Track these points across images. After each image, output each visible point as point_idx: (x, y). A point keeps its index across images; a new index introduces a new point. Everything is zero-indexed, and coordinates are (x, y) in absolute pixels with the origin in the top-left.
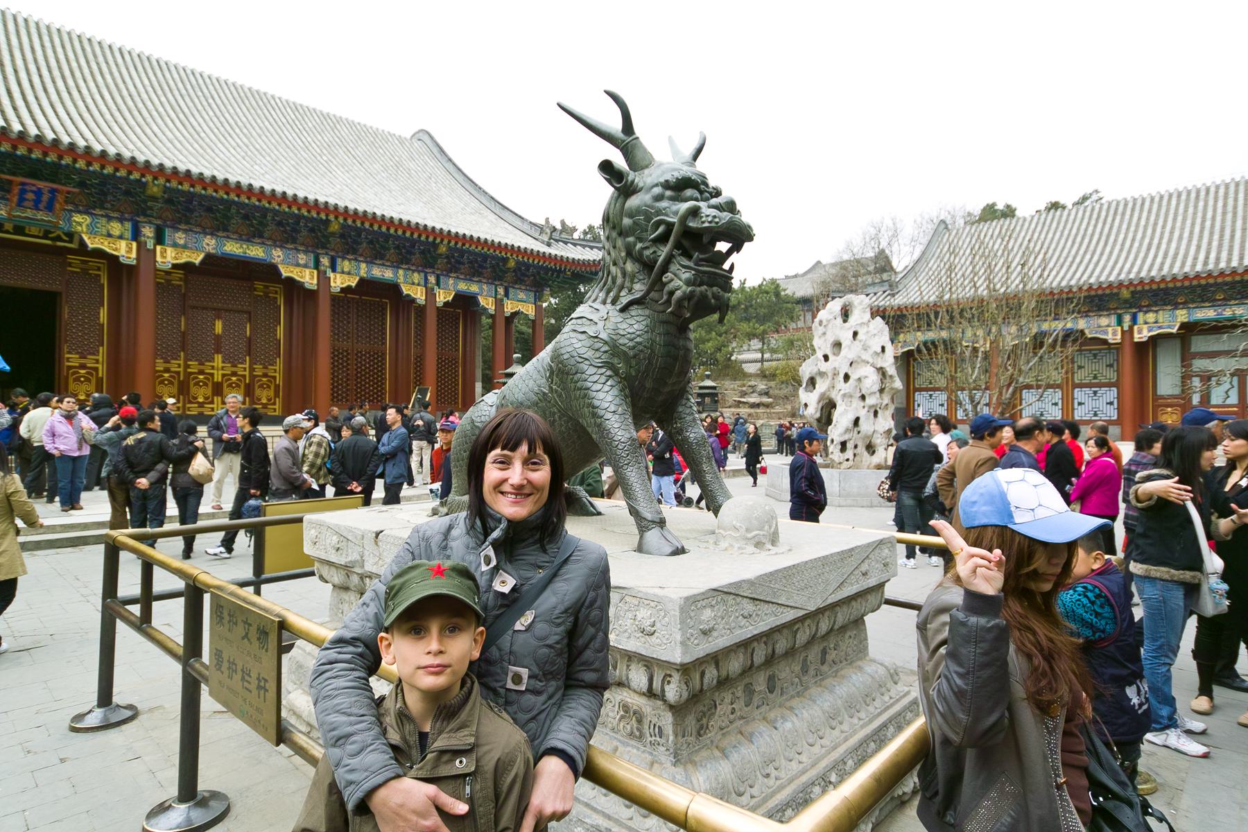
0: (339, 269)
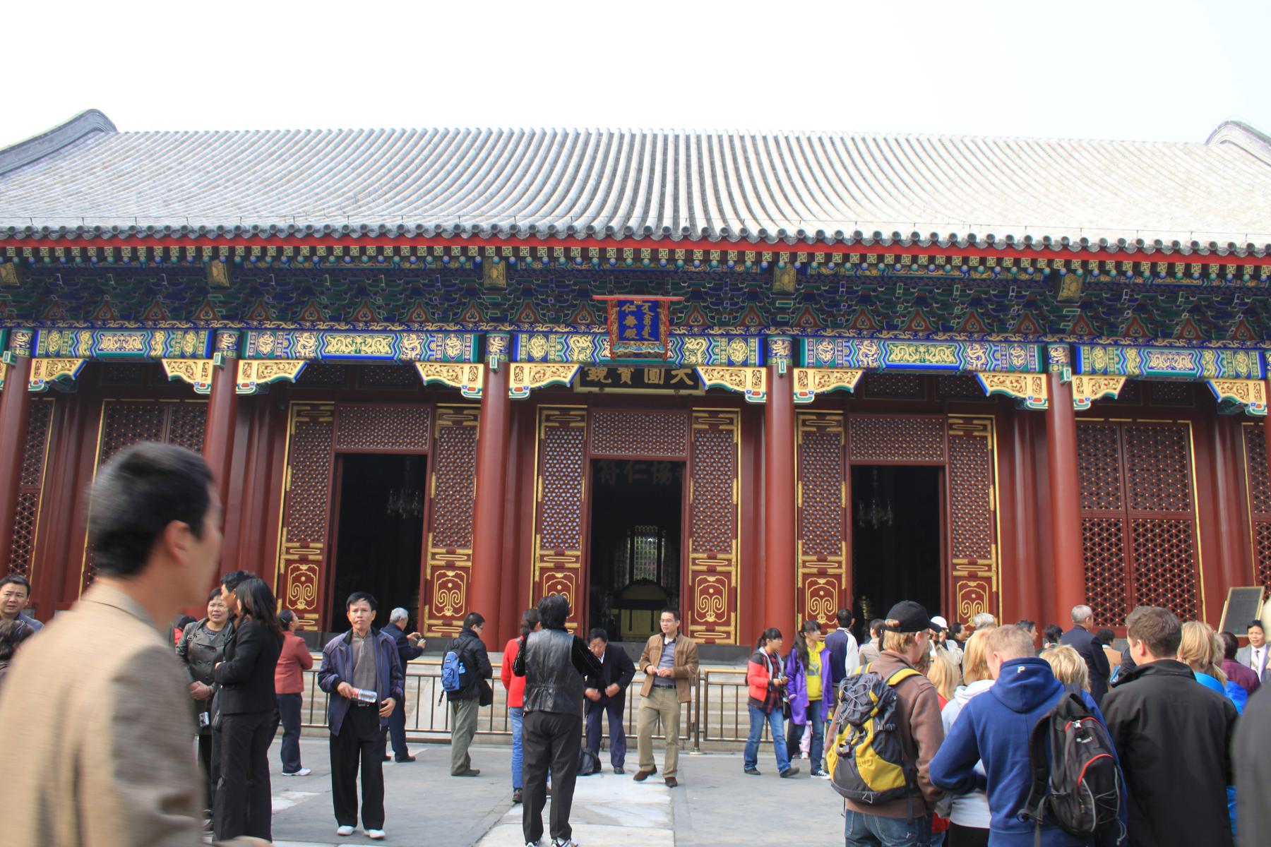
0: (1085, 367)
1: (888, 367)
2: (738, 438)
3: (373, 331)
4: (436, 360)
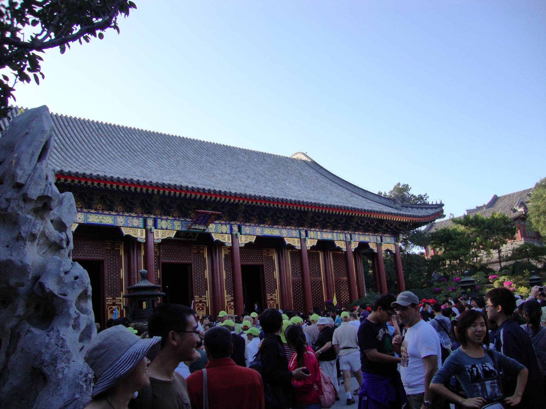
1: (88, 224)
2: (206, 255)
3: (105, 214)
4: (130, 227)
